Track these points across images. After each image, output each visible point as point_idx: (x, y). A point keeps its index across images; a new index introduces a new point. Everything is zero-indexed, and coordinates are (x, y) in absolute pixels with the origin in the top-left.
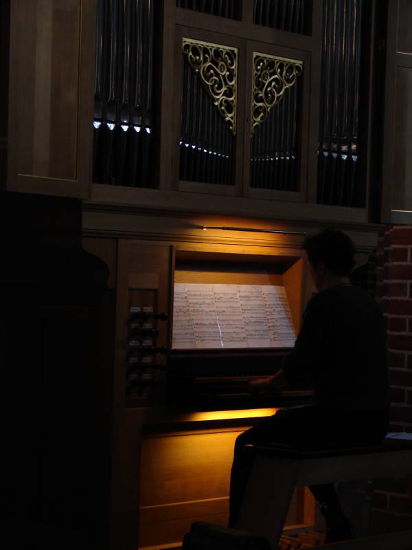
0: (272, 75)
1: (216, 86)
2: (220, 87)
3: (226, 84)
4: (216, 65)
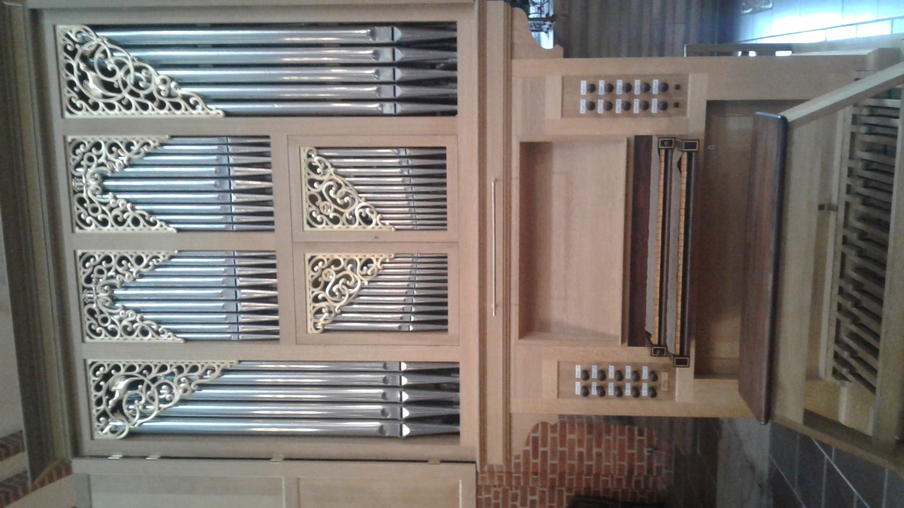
0: (324, 199)
1: (348, 283)
2: (348, 277)
3: (343, 269)
4: (327, 283)
